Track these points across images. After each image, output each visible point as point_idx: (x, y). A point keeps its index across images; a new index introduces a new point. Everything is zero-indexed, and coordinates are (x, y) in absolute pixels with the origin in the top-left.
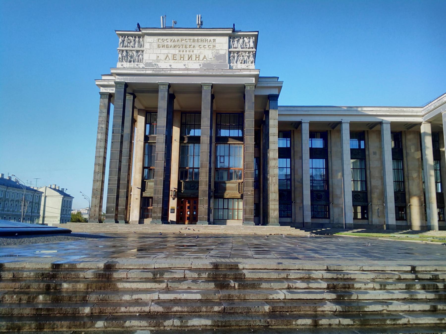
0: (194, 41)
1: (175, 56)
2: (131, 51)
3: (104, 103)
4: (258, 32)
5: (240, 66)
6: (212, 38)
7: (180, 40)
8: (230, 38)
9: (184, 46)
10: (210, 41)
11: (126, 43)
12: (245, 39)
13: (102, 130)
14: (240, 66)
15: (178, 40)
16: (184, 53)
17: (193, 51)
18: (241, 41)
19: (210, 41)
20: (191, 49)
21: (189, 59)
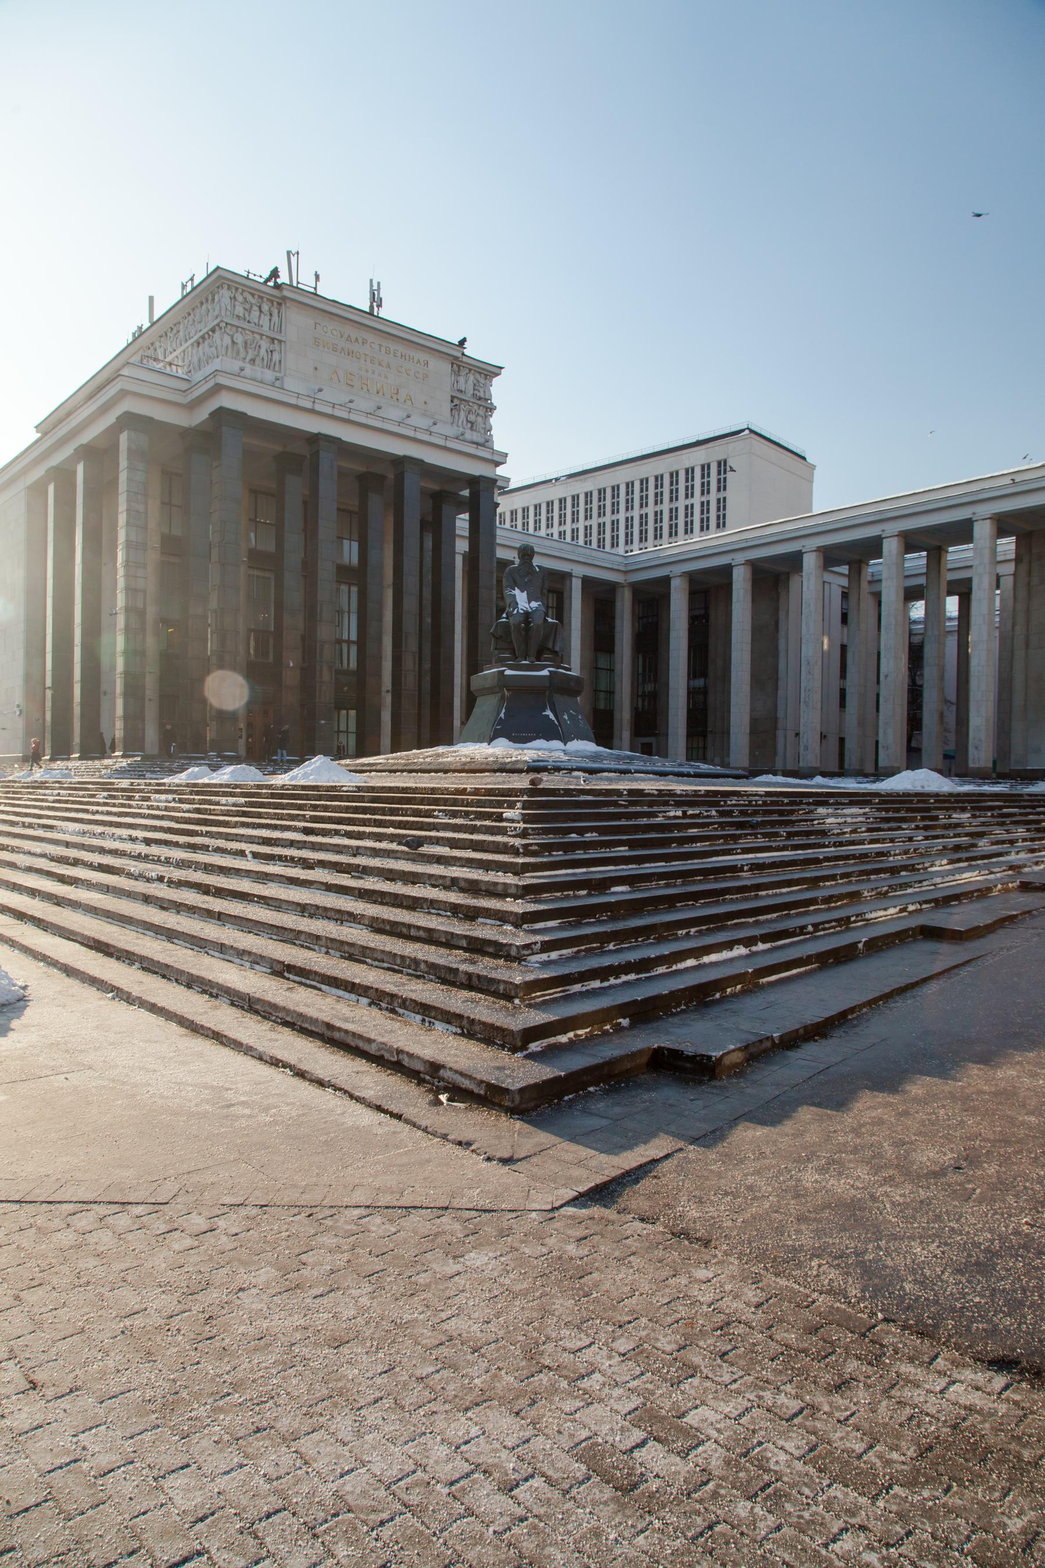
2: (253, 332)
5: (469, 435)
6: (423, 356)
7: (360, 341)
8: (452, 364)
10: (419, 362)
12: (478, 375)
14: (469, 435)
18: (471, 377)
19: (419, 362)
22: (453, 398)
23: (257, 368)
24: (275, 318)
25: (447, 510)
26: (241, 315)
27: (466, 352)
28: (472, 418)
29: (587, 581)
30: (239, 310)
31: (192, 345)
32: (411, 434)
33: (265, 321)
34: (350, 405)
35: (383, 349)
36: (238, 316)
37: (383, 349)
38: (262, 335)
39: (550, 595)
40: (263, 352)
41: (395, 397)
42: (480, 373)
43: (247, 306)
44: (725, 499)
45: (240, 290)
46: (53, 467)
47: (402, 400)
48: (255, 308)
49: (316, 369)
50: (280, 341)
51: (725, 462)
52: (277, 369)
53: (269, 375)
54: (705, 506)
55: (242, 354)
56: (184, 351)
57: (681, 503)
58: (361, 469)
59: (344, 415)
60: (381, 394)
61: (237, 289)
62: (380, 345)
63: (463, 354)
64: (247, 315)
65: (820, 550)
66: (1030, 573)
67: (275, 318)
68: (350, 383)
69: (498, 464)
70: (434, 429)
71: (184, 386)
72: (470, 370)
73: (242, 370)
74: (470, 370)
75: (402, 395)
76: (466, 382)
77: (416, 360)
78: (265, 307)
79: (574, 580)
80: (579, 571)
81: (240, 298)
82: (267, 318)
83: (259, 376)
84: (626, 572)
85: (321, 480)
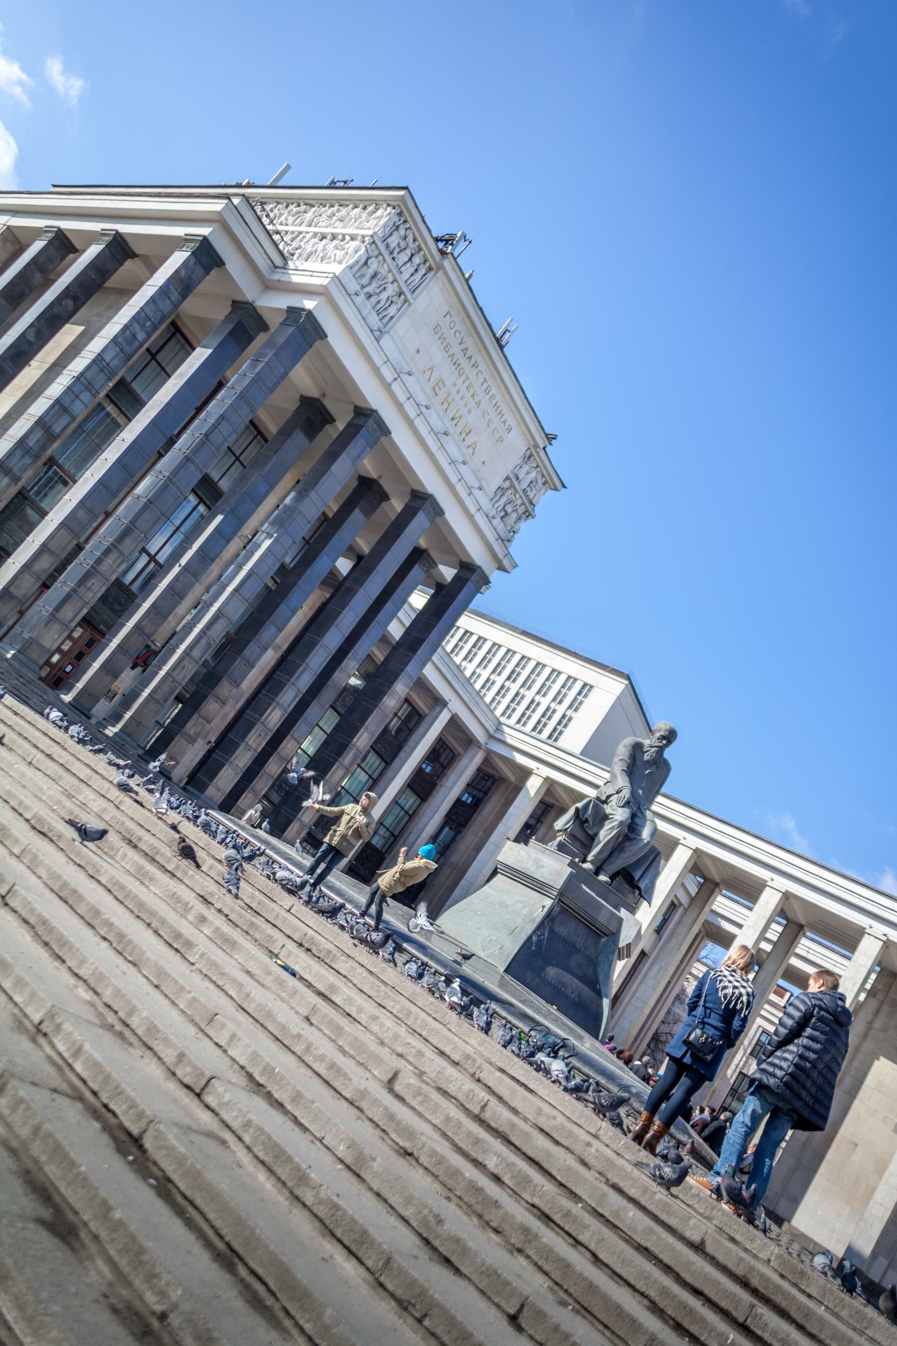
0: (487, 391)
1: (440, 384)
3: (190, 277)
4: (564, 487)
6: (512, 422)
9: (467, 384)
10: (505, 422)
11: (394, 241)
12: (540, 476)
13: (130, 344)
15: (470, 358)
16: (458, 398)
17: (469, 411)
20: (472, 404)
21: (452, 419)
22: (508, 478)
23: (368, 305)
24: (418, 277)
25: (417, 571)
26: (392, 246)
27: (548, 449)
28: (509, 509)
29: (454, 723)
30: (394, 241)
31: (315, 235)
32: (454, 479)
33: (408, 270)
34: (424, 410)
35: (485, 385)
36: (388, 246)
37: (485, 385)
38: (395, 280)
39: (406, 705)
40: (384, 296)
41: (464, 435)
42: (543, 476)
43: (403, 244)
44: (570, 719)
45: (407, 225)
46: (59, 229)
47: (467, 443)
48: (408, 252)
49: (418, 351)
50: (406, 301)
51: (591, 687)
52: (385, 321)
53: (374, 320)
54: (548, 713)
55: (365, 281)
56: (300, 233)
57: (529, 695)
58: (374, 475)
59: (412, 413)
60: (455, 422)
61: (405, 222)
62: (485, 380)
63: (544, 448)
64: (397, 250)
65: (697, 852)
66: (877, 1013)
67: (418, 277)
68: (437, 389)
69: (501, 568)
70: (476, 492)
71: (278, 261)
72: (538, 466)
73: (356, 294)
74: (538, 466)
75: (470, 440)
76: (528, 475)
77: (503, 419)
78: (417, 260)
79: (445, 710)
80: (455, 706)
81: (402, 232)
82: (412, 270)
83: (365, 312)
84: (491, 736)
85: (344, 456)
